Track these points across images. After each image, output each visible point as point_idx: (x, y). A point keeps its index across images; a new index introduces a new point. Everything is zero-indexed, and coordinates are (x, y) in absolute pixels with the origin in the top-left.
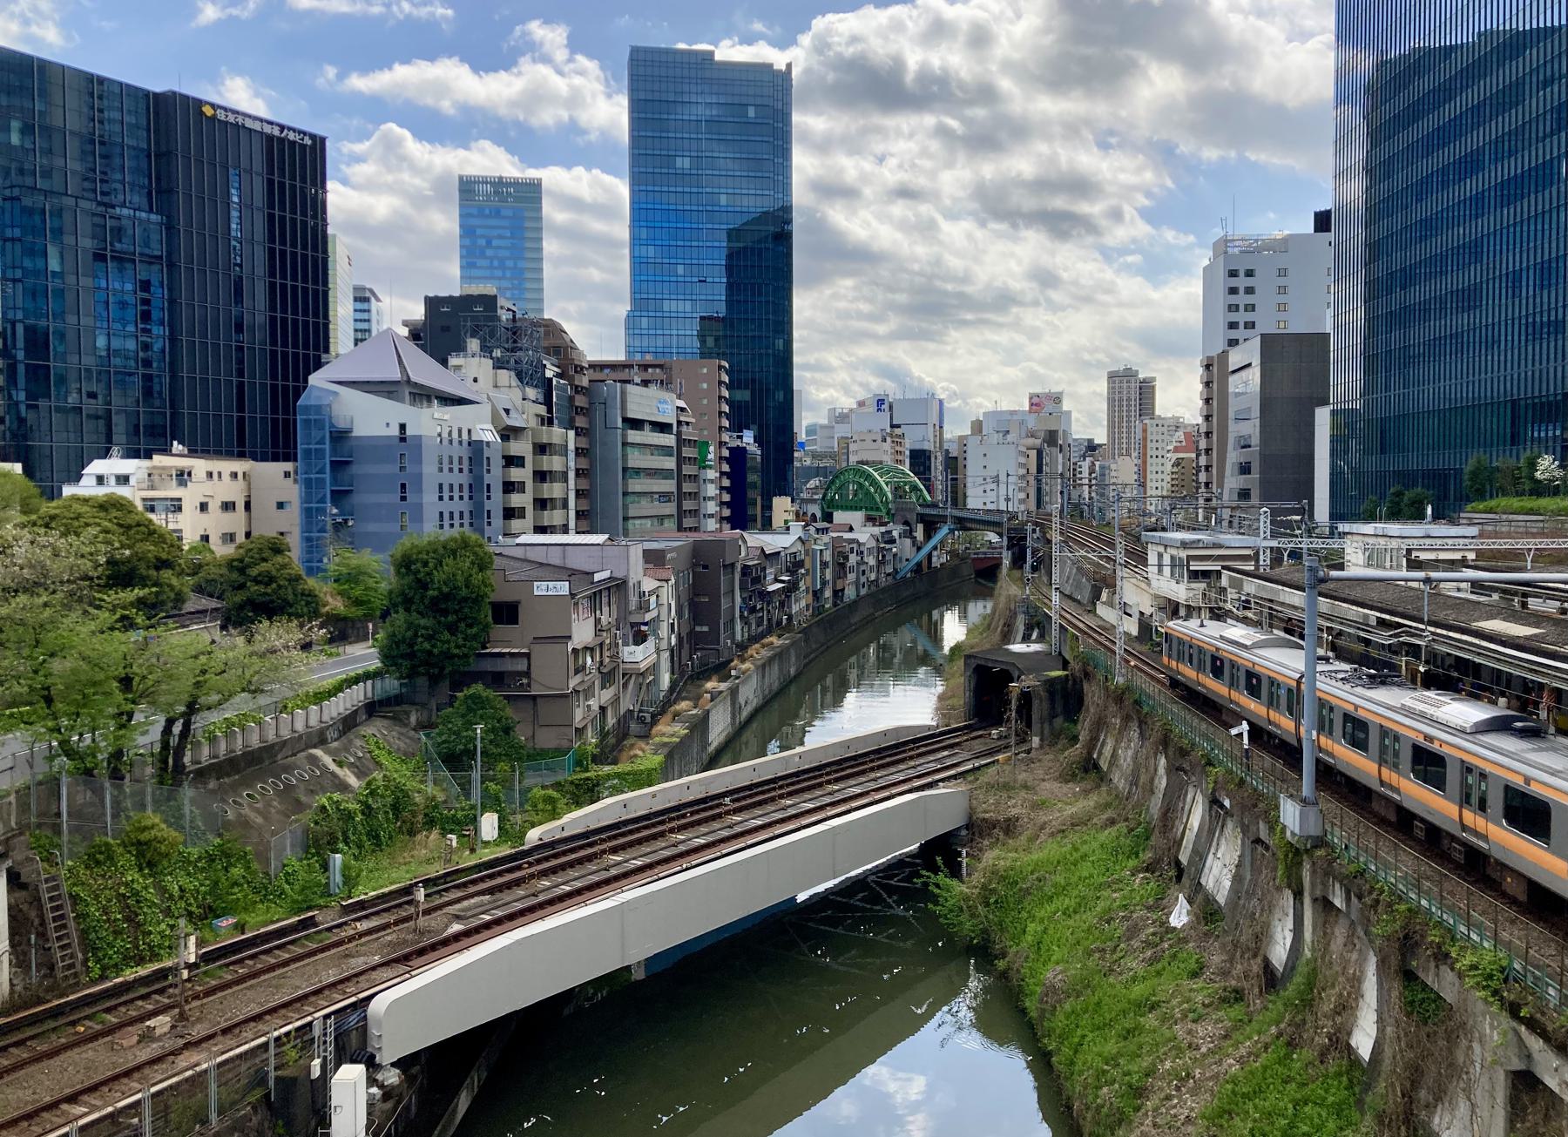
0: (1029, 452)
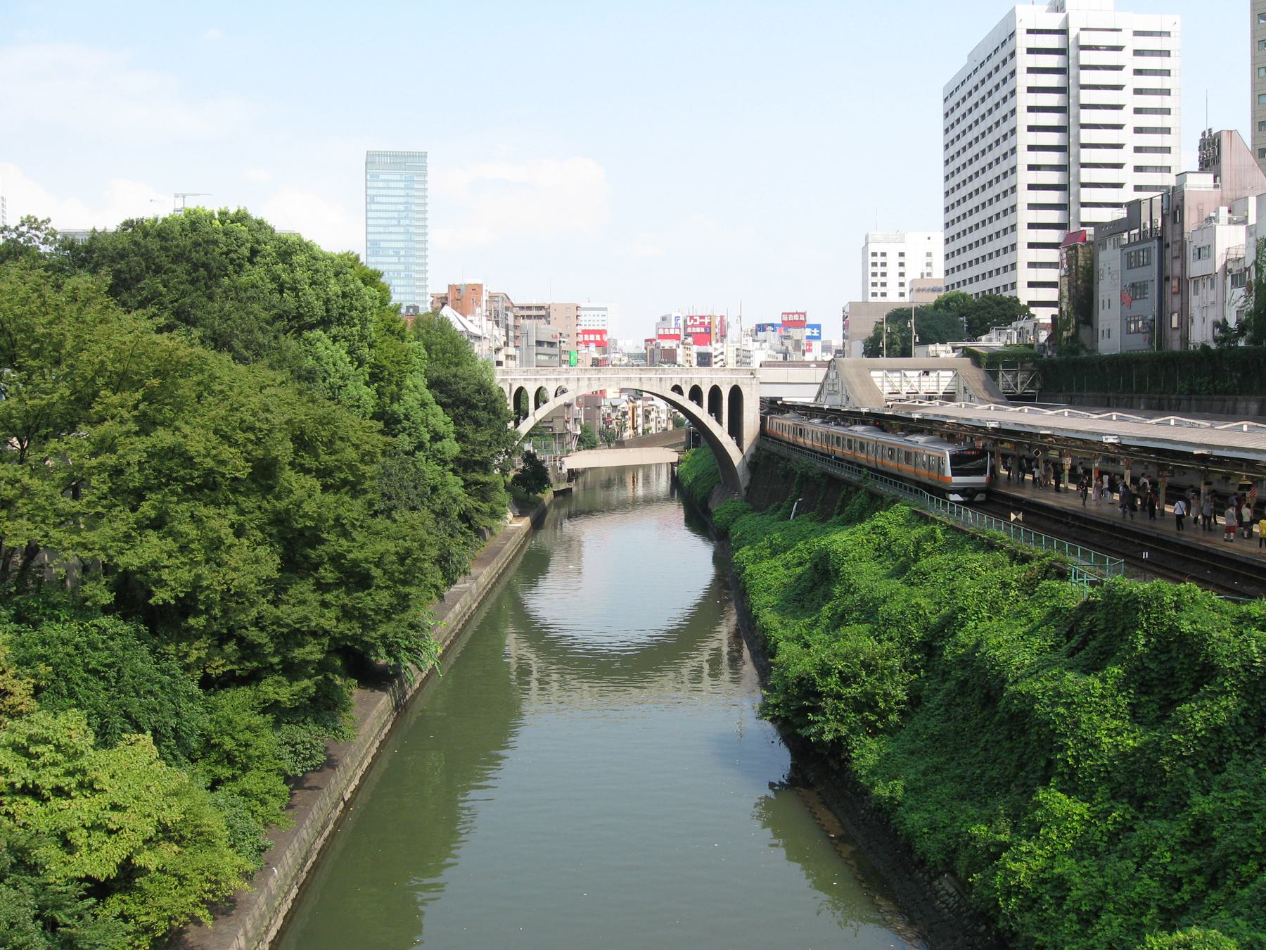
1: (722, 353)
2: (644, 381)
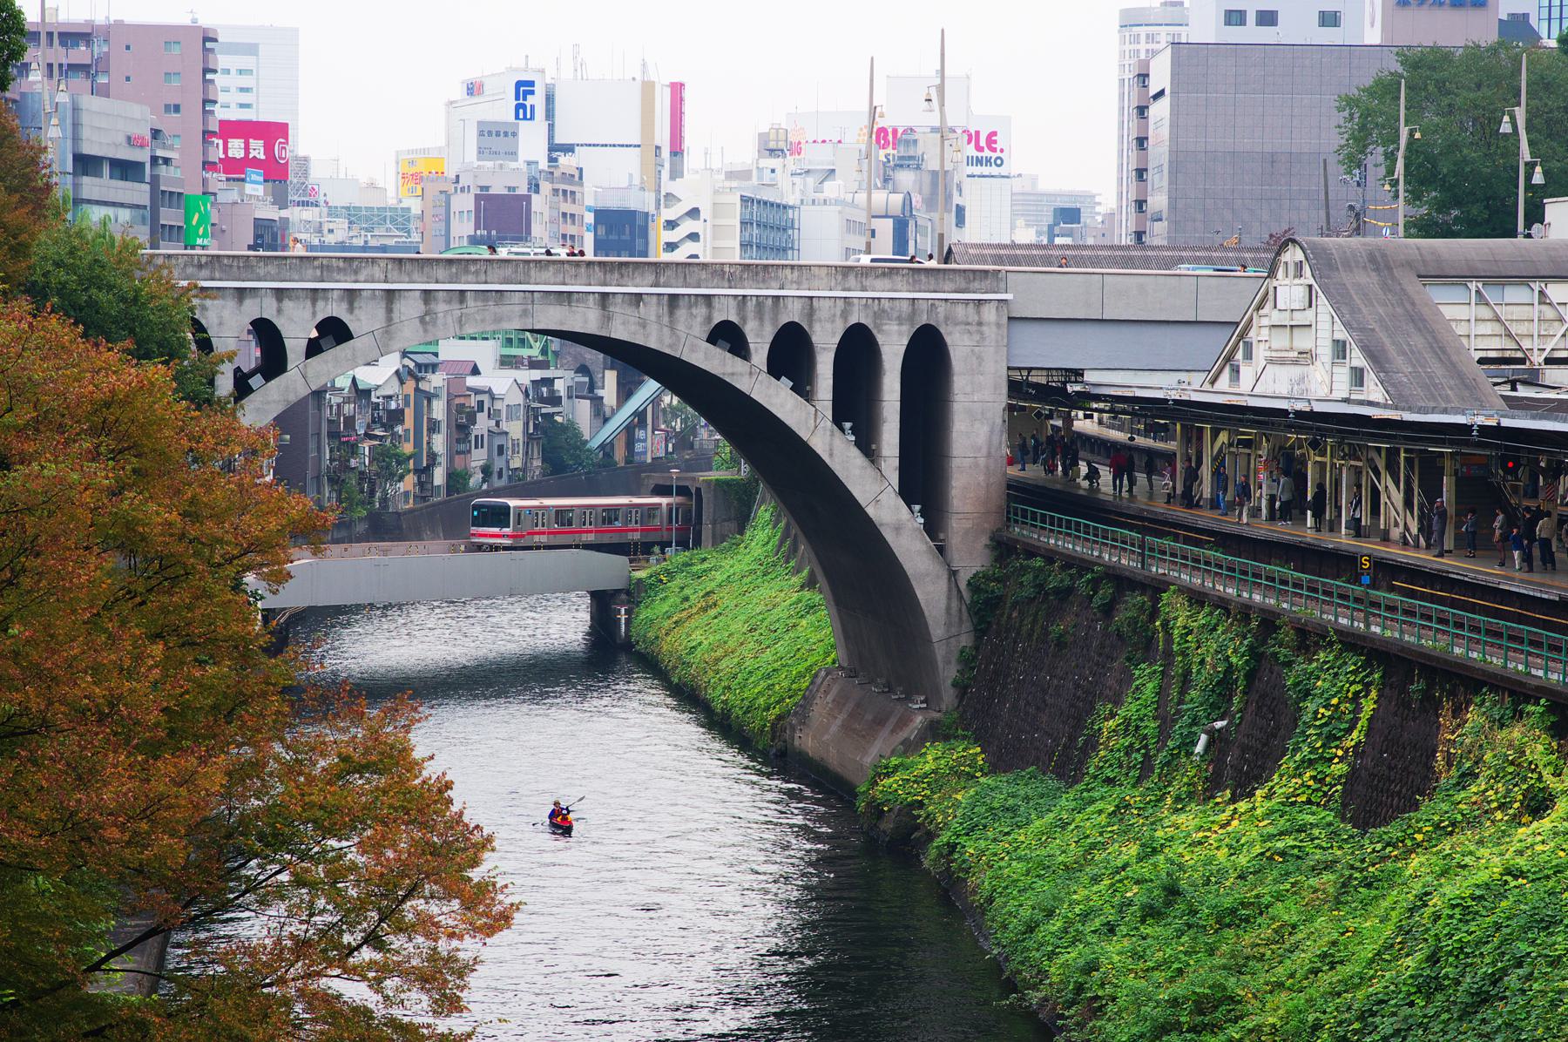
0: (877, 224)
1: (694, 213)
2: (617, 308)
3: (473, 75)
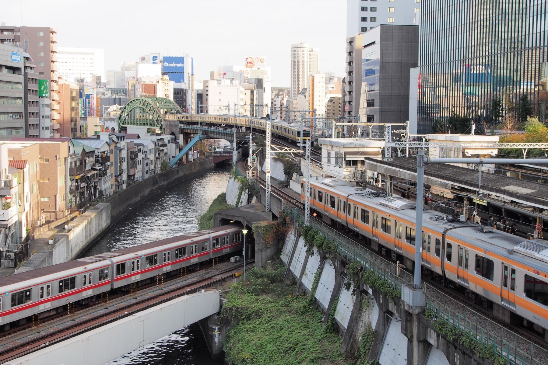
3: (142, 56)
